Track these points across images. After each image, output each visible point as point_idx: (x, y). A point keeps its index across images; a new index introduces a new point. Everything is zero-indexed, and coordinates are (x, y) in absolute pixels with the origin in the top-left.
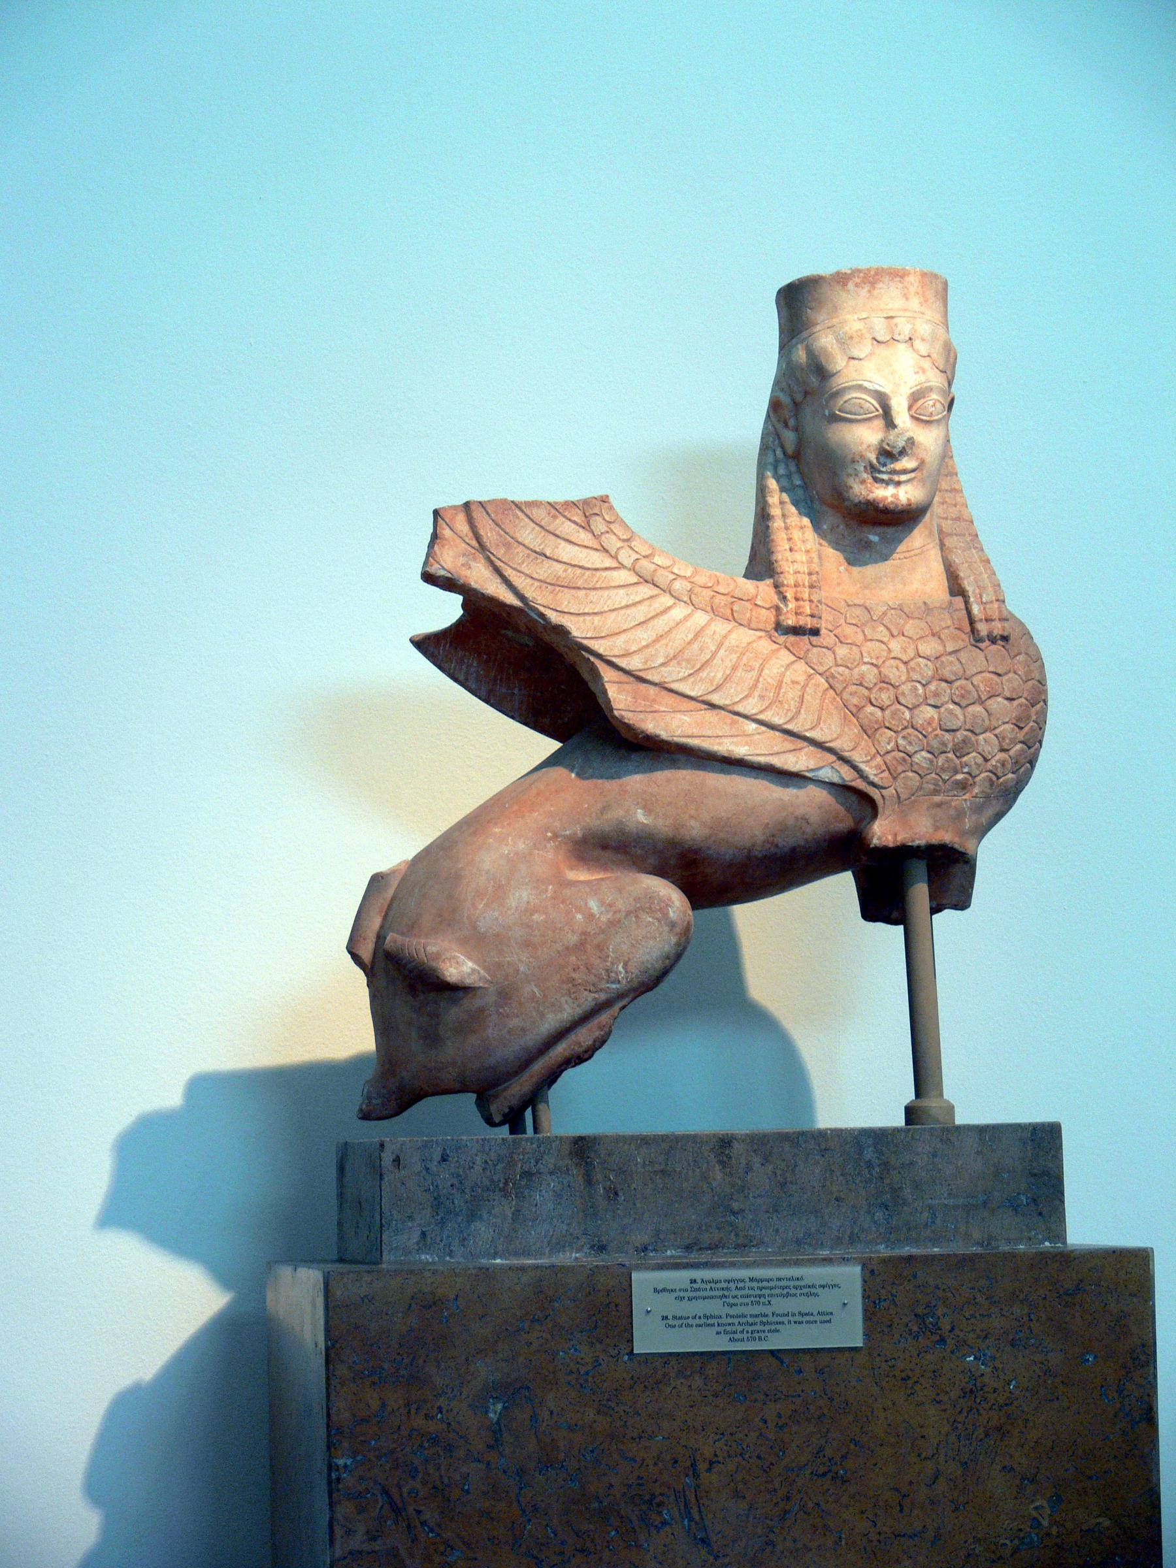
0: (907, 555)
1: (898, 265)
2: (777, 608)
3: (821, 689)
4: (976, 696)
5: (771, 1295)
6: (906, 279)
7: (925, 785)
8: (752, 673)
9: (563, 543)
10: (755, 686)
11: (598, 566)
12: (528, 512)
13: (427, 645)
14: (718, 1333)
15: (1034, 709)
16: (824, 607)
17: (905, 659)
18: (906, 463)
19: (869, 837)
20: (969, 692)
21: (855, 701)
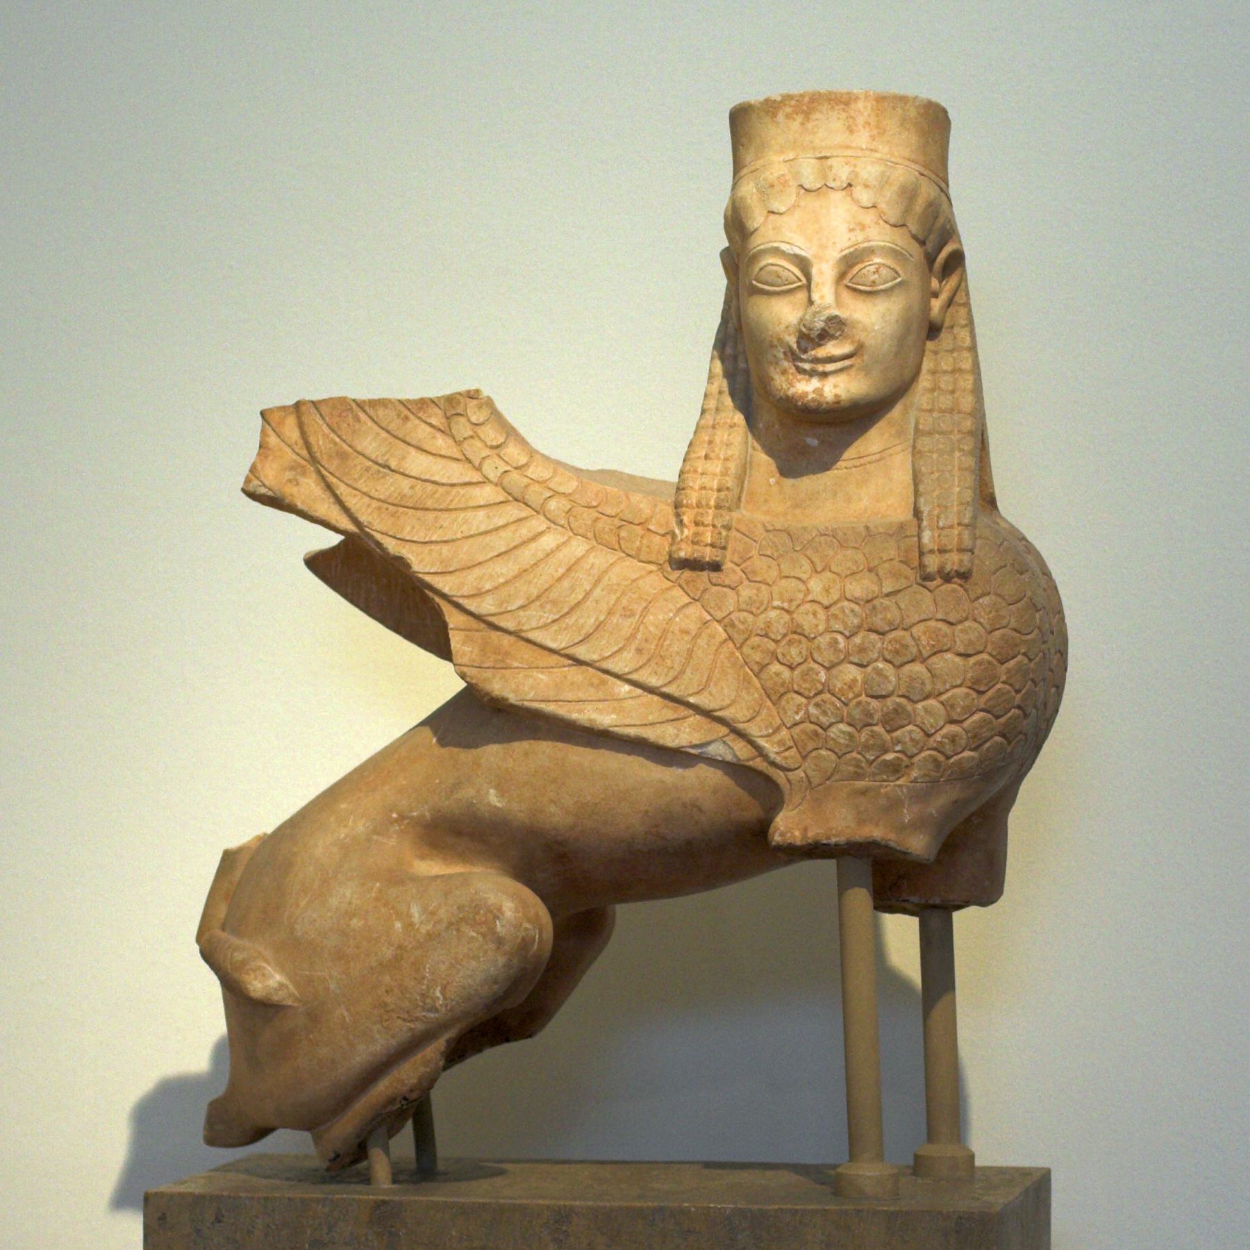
0: (857, 462)
1: (841, 87)
2: (674, 535)
4: (914, 650)
6: (853, 106)
7: (843, 768)
8: (630, 620)
9: (413, 451)
10: (633, 636)
11: (455, 481)
12: (372, 413)
13: (318, 563)
16: (734, 533)
17: (826, 603)
18: (832, 348)
20: (906, 647)
21: (757, 656)
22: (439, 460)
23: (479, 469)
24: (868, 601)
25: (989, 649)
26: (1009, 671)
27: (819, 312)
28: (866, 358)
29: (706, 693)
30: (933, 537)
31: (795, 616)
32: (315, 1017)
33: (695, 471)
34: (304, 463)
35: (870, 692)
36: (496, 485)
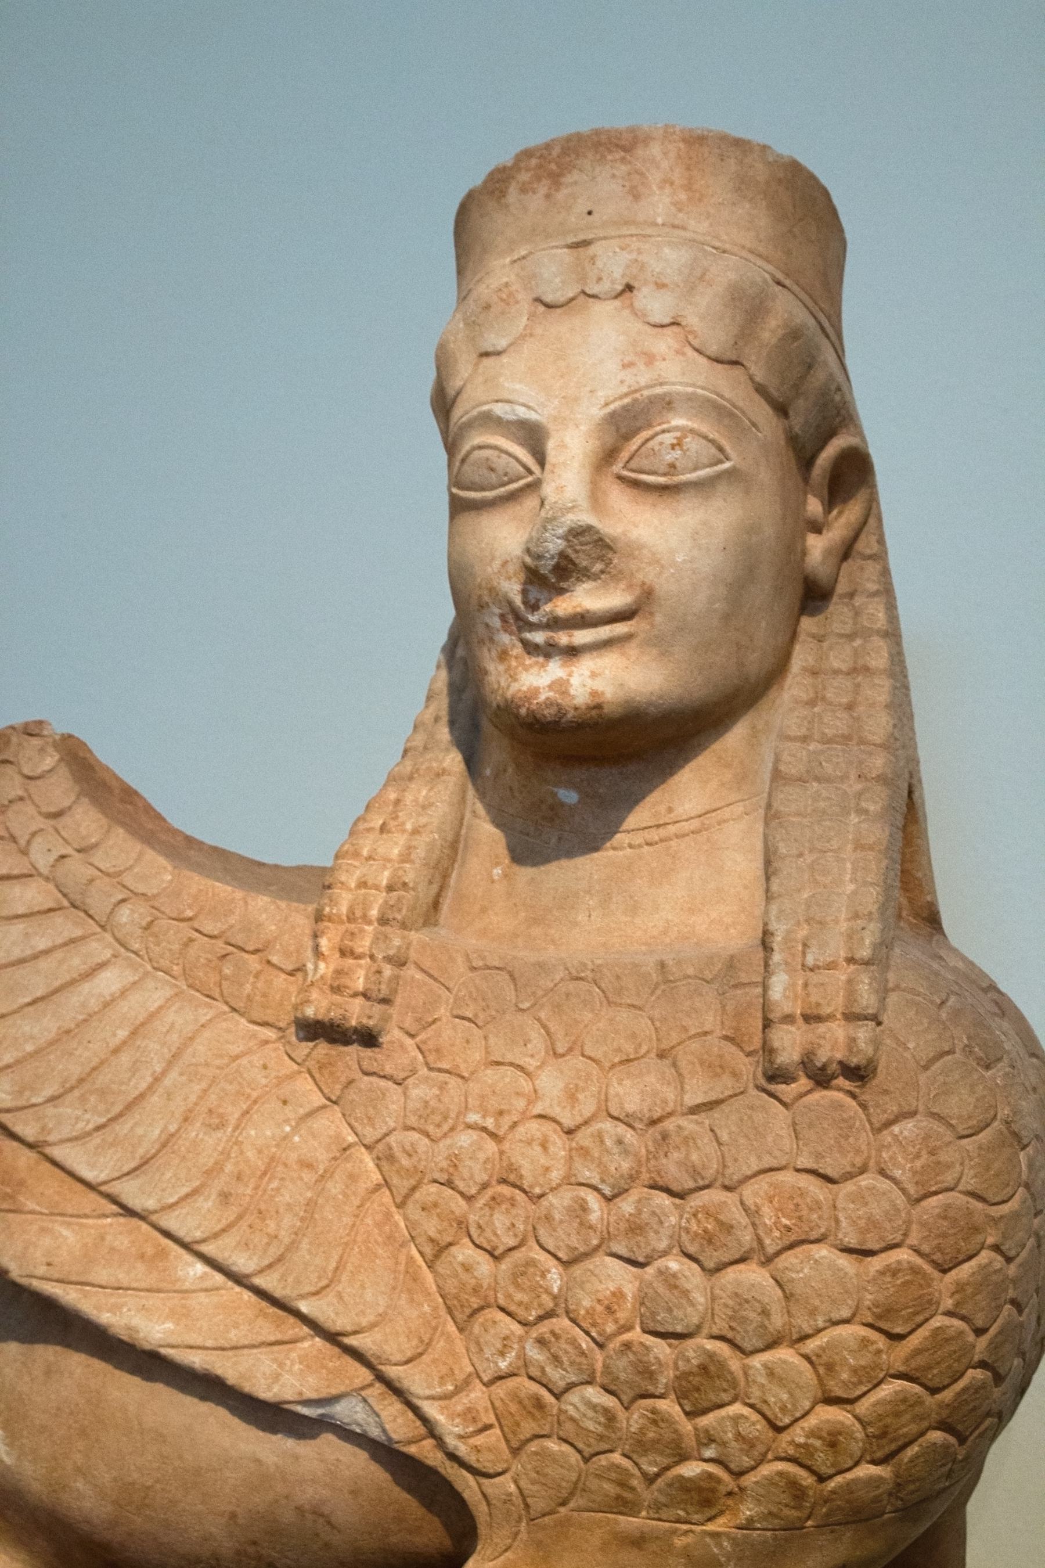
0: (654, 835)
3: (363, 1186)
6: (640, 152)
7: (593, 1483)
8: (219, 1134)
17: (568, 1122)
18: (584, 598)
20: (728, 1228)
21: (431, 1226)
23: (25, 852)
24: (653, 1122)
25: (913, 1239)
26: (960, 1288)
27: (554, 518)
28: (658, 618)
29: (330, 1297)
31: (506, 1146)
35: (651, 1326)
36: (47, 879)
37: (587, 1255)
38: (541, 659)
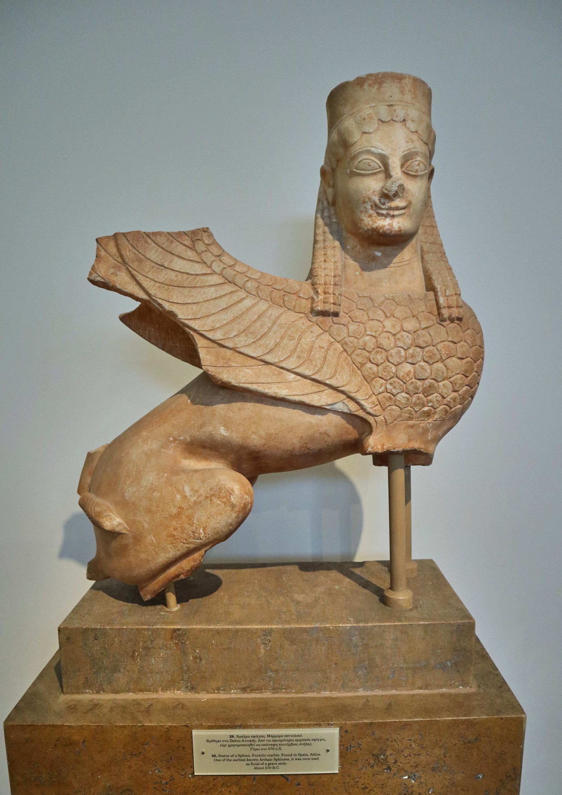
0: (399, 264)
2: (313, 299)
4: (439, 356)
5: (282, 745)
7: (403, 414)
9: (176, 259)
10: (295, 350)
11: (198, 273)
12: (154, 239)
14: (247, 764)
15: (476, 364)
16: (343, 298)
17: (394, 333)
18: (398, 203)
19: (366, 446)
22: (189, 262)
23: (210, 267)
24: (415, 332)
27: (396, 181)
28: (411, 209)
30: (444, 300)
31: (378, 339)
32: (138, 539)
33: (321, 268)
34: (119, 265)
35: (418, 378)
37: (401, 363)
38: (384, 218)
